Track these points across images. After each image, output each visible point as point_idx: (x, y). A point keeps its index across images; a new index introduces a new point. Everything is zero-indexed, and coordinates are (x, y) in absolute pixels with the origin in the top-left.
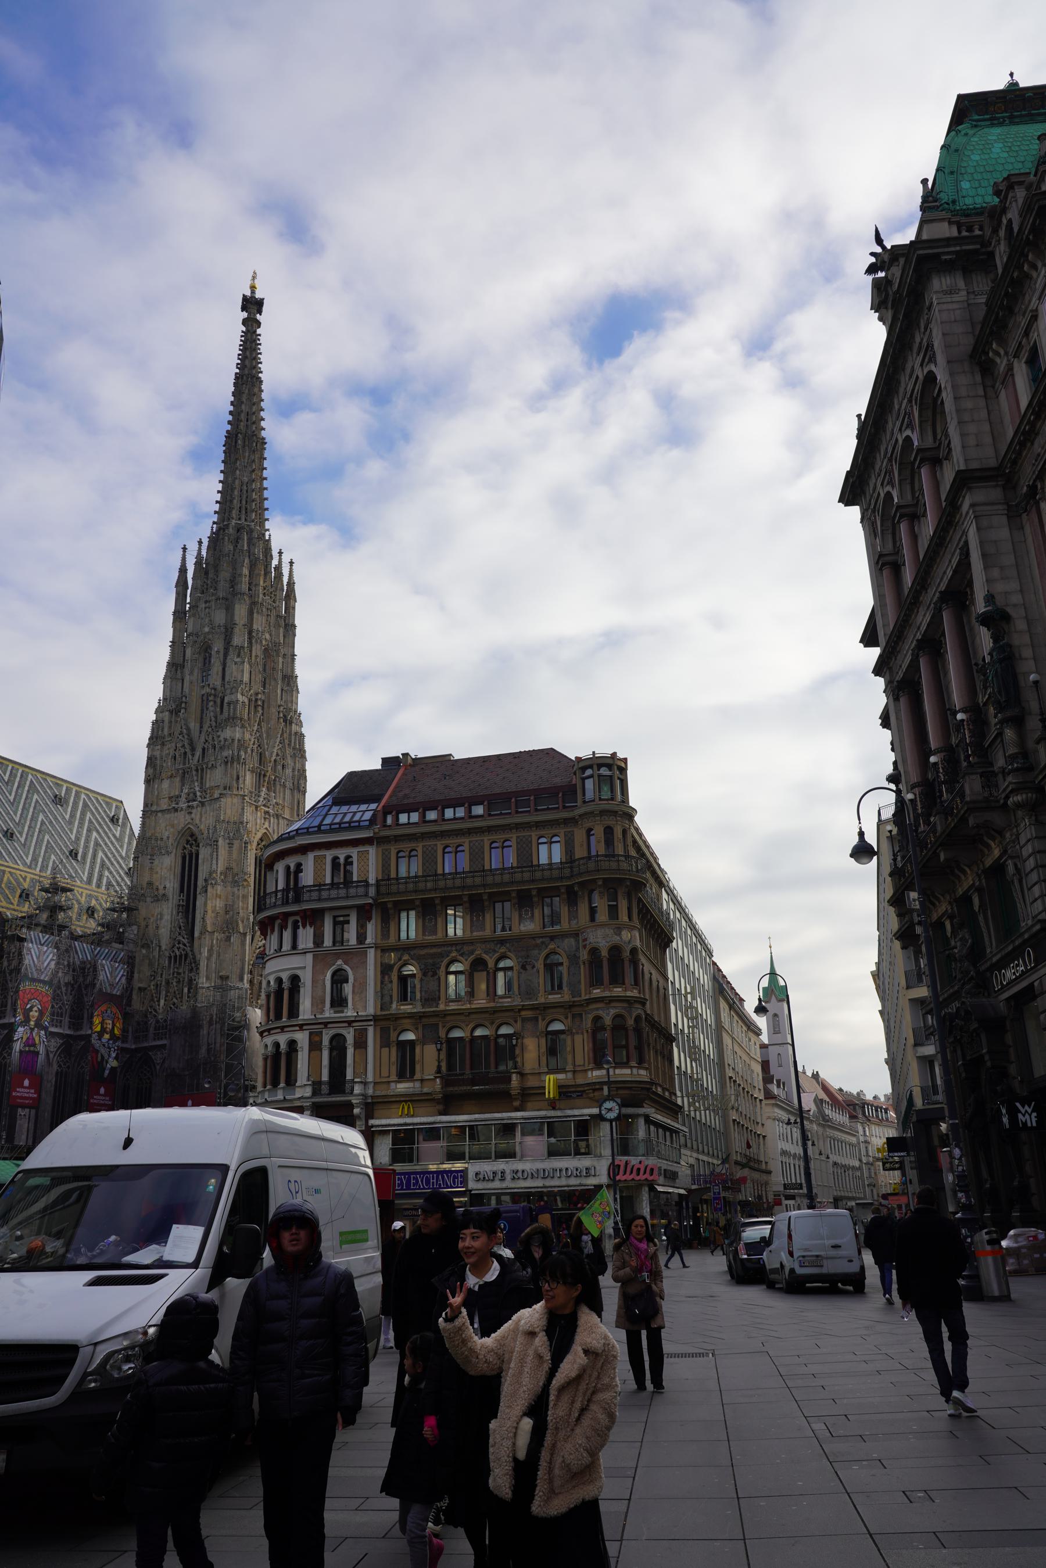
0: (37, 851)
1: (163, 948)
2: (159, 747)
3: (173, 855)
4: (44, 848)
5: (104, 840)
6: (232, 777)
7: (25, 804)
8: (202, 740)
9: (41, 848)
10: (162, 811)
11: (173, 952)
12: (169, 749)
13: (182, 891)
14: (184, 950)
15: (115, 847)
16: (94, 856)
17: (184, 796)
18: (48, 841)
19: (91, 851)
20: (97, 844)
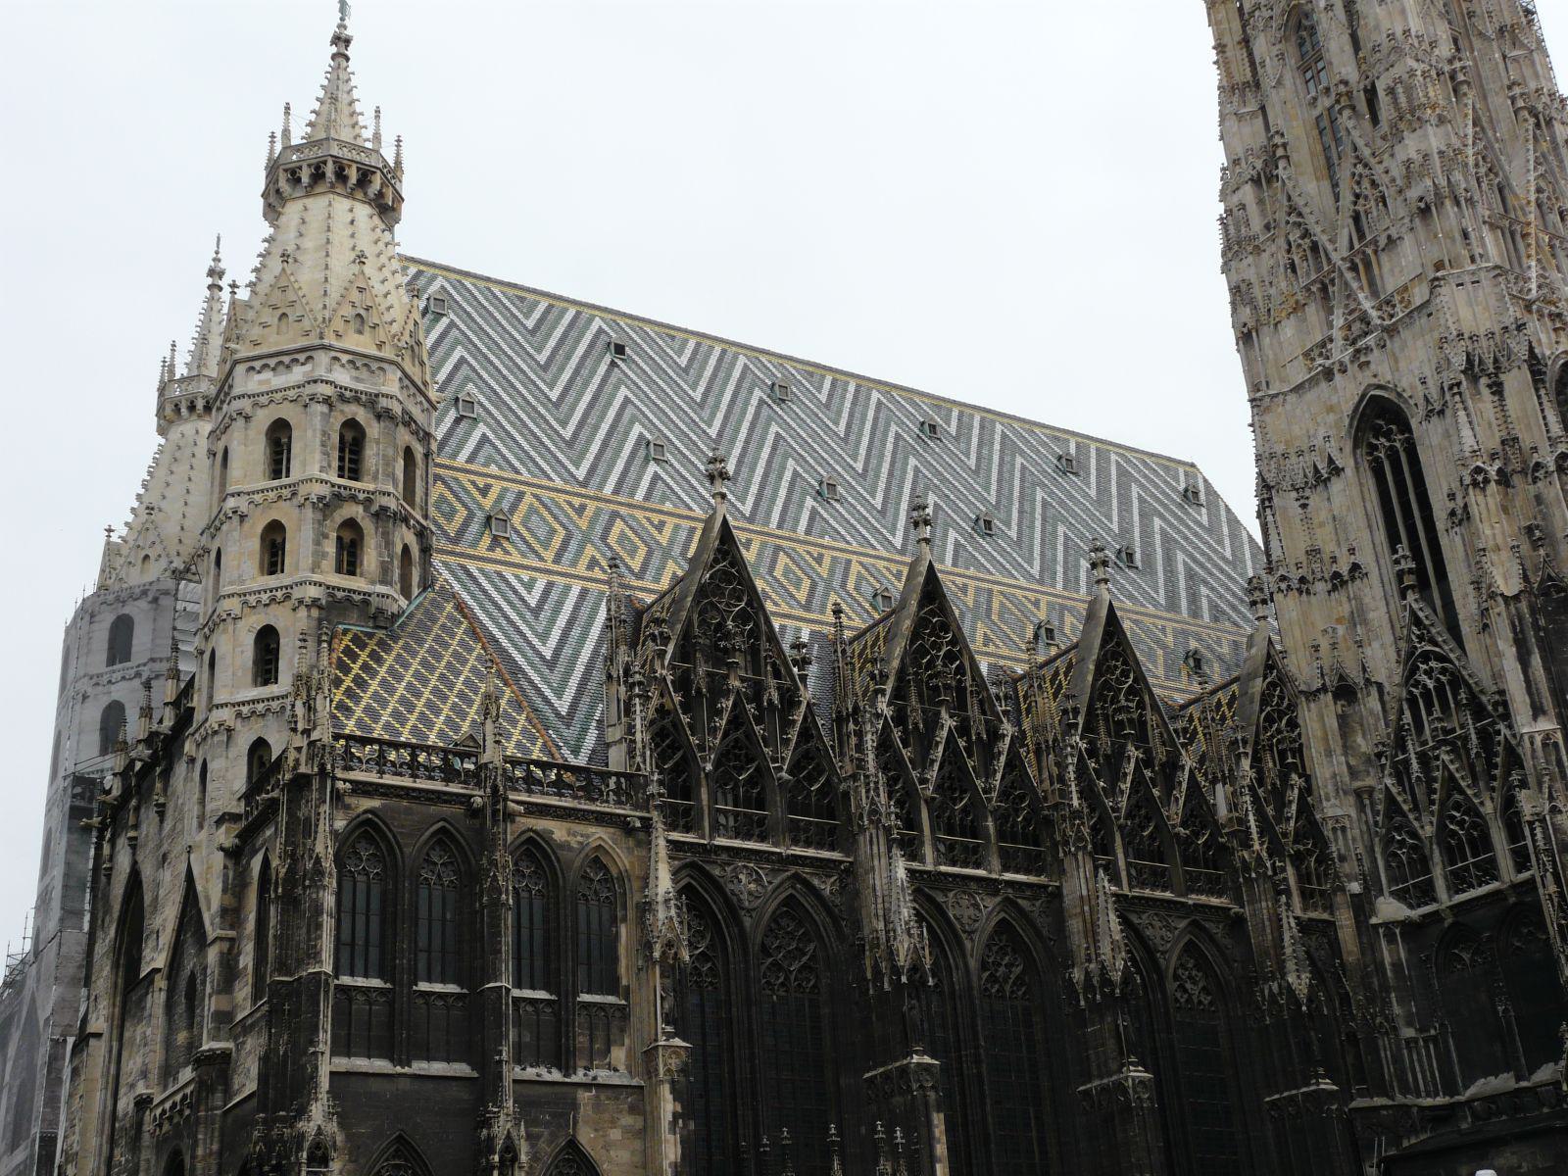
0: (1049, 554)
1: (1387, 688)
2: (1250, 259)
3: (1349, 472)
4: (1060, 548)
5: (1179, 532)
6: (1447, 236)
7: (1000, 473)
8: (1347, 198)
9: (1055, 549)
10: (1298, 389)
11: (1417, 684)
12: (1274, 255)
13: (1393, 540)
14: (1444, 671)
15: (1206, 543)
16: (1169, 559)
17: (1337, 334)
18: (1065, 534)
19: (1159, 550)
20: (1166, 539)
